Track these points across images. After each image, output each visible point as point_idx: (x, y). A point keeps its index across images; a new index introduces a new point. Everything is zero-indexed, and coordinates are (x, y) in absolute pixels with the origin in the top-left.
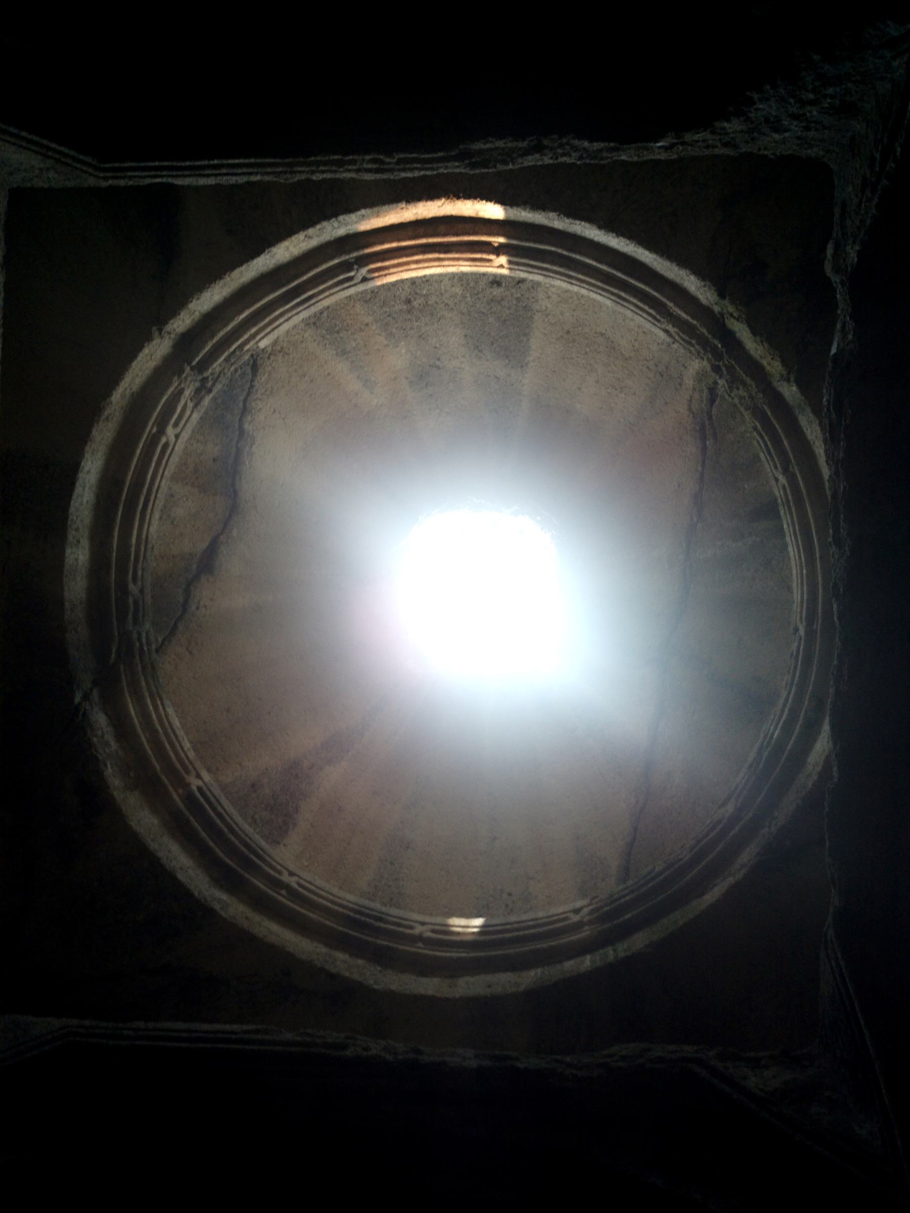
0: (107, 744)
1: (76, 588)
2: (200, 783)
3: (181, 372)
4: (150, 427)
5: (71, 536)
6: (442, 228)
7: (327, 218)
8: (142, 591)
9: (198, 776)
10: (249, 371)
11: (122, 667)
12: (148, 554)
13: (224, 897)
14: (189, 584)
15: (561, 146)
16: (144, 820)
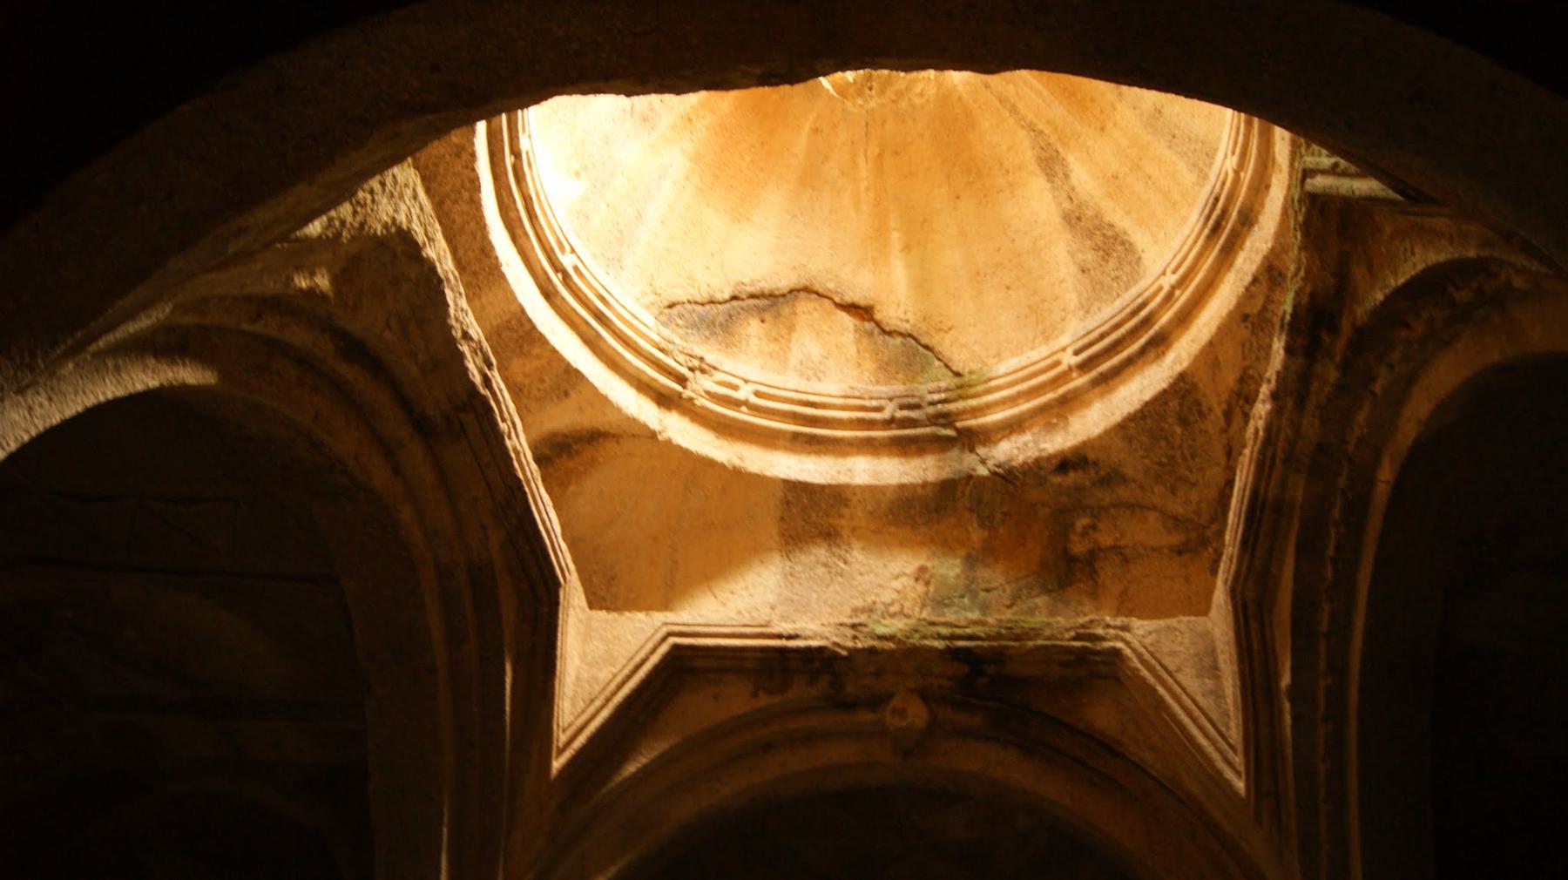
0: (1025, 444)
1: (891, 471)
2: (1070, 351)
3: (691, 399)
4: (743, 415)
5: (843, 479)
6: (512, 215)
7: (534, 328)
8: (891, 399)
9: (1064, 349)
10: (674, 311)
11: (959, 424)
12: (857, 393)
13: (1171, 356)
14: (884, 332)
15: (457, 320)
16: (1094, 420)
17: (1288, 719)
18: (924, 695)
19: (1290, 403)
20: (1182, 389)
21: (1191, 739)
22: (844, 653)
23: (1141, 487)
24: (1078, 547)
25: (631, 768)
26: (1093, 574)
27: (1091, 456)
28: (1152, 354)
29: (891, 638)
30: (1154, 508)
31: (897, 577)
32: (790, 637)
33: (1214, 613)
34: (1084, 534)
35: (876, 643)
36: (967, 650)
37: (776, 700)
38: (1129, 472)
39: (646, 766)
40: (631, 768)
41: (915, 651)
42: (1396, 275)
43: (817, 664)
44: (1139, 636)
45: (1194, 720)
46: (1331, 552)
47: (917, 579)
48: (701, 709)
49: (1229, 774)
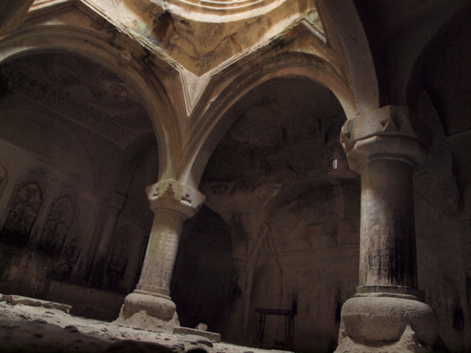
0: (178, 10)
17: (207, 107)
18: (132, 54)
19: (260, 53)
20: (221, 26)
21: (184, 99)
22: (120, 32)
23: (195, 39)
24: (172, 42)
25: (49, 23)
26: (172, 50)
27: (191, 24)
28: (220, 13)
29: (133, 36)
30: (193, 45)
31: (129, 18)
32: (109, 18)
33: (202, 77)
34: (175, 39)
35: (129, 35)
36: (149, 51)
37: (96, 31)
38: (195, 33)
39: (53, 25)
40: (49, 23)
41: (136, 43)
42: (306, 50)
43: (111, 29)
44: (184, 72)
45: (186, 96)
46: (242, 83)
47: (133, 22)
48: (74, 20)
49: (187, 111)
